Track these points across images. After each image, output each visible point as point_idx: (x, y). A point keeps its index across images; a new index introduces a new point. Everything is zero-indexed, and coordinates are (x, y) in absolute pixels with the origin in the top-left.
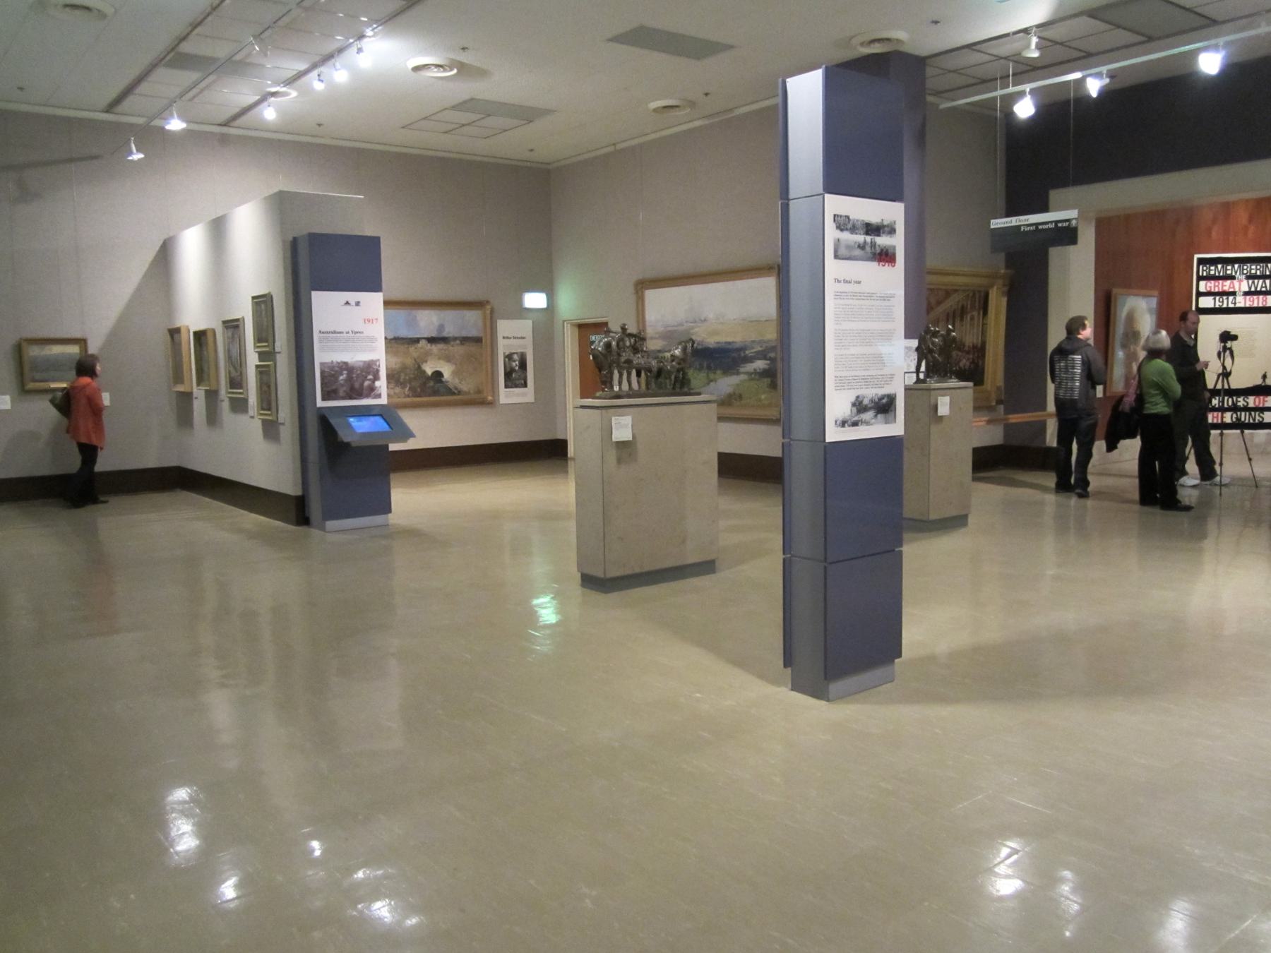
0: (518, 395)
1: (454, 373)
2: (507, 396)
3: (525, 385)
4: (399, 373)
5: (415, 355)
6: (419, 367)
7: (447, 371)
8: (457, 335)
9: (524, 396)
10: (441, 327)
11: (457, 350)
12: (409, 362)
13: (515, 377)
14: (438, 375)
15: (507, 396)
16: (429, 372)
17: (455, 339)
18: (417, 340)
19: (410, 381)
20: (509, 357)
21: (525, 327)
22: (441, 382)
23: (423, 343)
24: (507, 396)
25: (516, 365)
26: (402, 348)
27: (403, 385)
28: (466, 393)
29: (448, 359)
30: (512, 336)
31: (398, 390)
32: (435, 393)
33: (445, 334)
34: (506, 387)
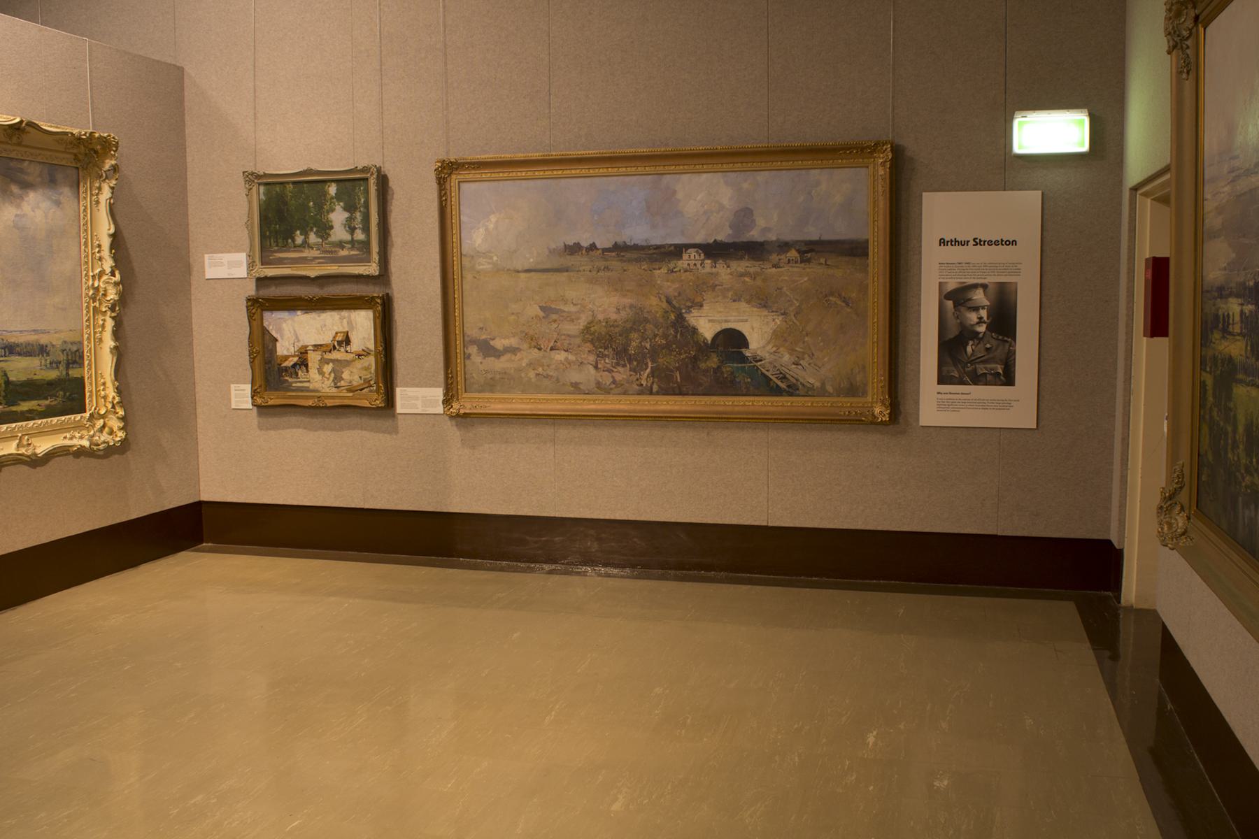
0: (983, 405)
1: (779, 337)
2: (942, 407)
3: (1008, 378)
4: (626, 333)
5: (671, 288)
6: (680, 318)
7: (758, 332)
8: (789, 237)
9: (1012, 407)
10: (744, 216)
11: (789, 275)
12: (654, 304)
13: (980, 346)
14: (732, 341)
15: (942, 407)
16: (707, 330)
17: (784, 246)
18: (677, 251)
19: (654, 353)
20: (958, 297)
21: (1020, 210)
22: (744, 359)
23: (690, 257)
24: (936, 404)
25: (978, 319)
26: (633, 269)
27: (634, 360)
28: (809, 392)
29: (763, 300)
30: (966, 238)
31: (622, 374)
32: (726, 386)
33: (755, 235)
34: (942, 380)
